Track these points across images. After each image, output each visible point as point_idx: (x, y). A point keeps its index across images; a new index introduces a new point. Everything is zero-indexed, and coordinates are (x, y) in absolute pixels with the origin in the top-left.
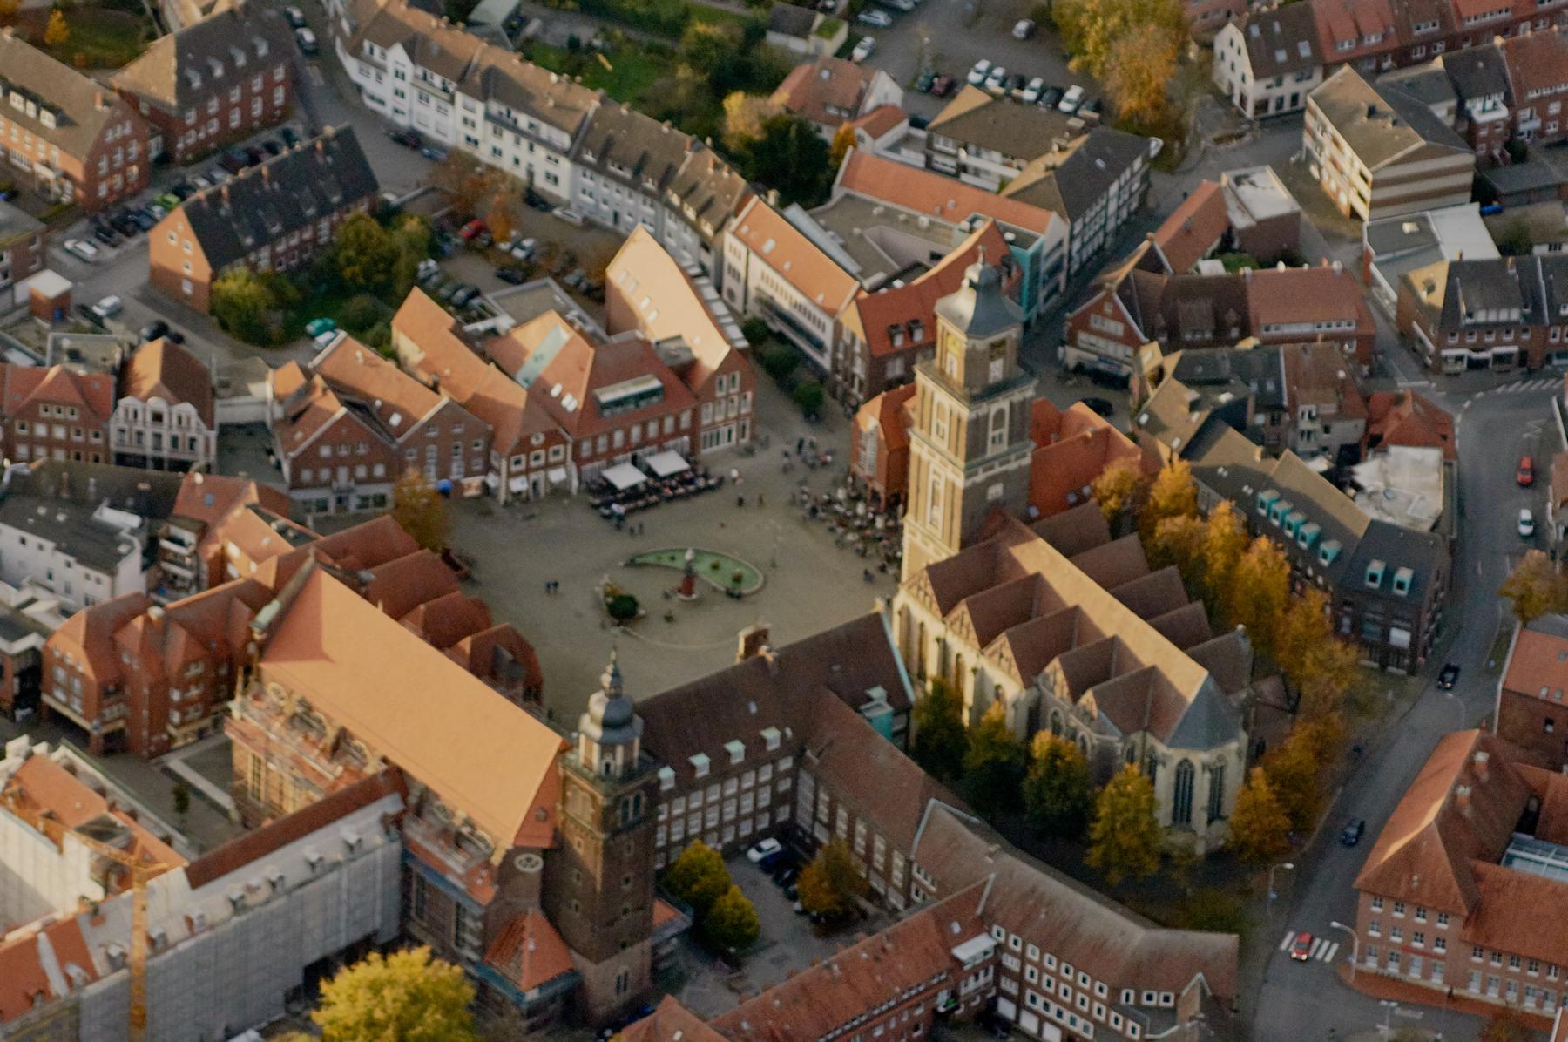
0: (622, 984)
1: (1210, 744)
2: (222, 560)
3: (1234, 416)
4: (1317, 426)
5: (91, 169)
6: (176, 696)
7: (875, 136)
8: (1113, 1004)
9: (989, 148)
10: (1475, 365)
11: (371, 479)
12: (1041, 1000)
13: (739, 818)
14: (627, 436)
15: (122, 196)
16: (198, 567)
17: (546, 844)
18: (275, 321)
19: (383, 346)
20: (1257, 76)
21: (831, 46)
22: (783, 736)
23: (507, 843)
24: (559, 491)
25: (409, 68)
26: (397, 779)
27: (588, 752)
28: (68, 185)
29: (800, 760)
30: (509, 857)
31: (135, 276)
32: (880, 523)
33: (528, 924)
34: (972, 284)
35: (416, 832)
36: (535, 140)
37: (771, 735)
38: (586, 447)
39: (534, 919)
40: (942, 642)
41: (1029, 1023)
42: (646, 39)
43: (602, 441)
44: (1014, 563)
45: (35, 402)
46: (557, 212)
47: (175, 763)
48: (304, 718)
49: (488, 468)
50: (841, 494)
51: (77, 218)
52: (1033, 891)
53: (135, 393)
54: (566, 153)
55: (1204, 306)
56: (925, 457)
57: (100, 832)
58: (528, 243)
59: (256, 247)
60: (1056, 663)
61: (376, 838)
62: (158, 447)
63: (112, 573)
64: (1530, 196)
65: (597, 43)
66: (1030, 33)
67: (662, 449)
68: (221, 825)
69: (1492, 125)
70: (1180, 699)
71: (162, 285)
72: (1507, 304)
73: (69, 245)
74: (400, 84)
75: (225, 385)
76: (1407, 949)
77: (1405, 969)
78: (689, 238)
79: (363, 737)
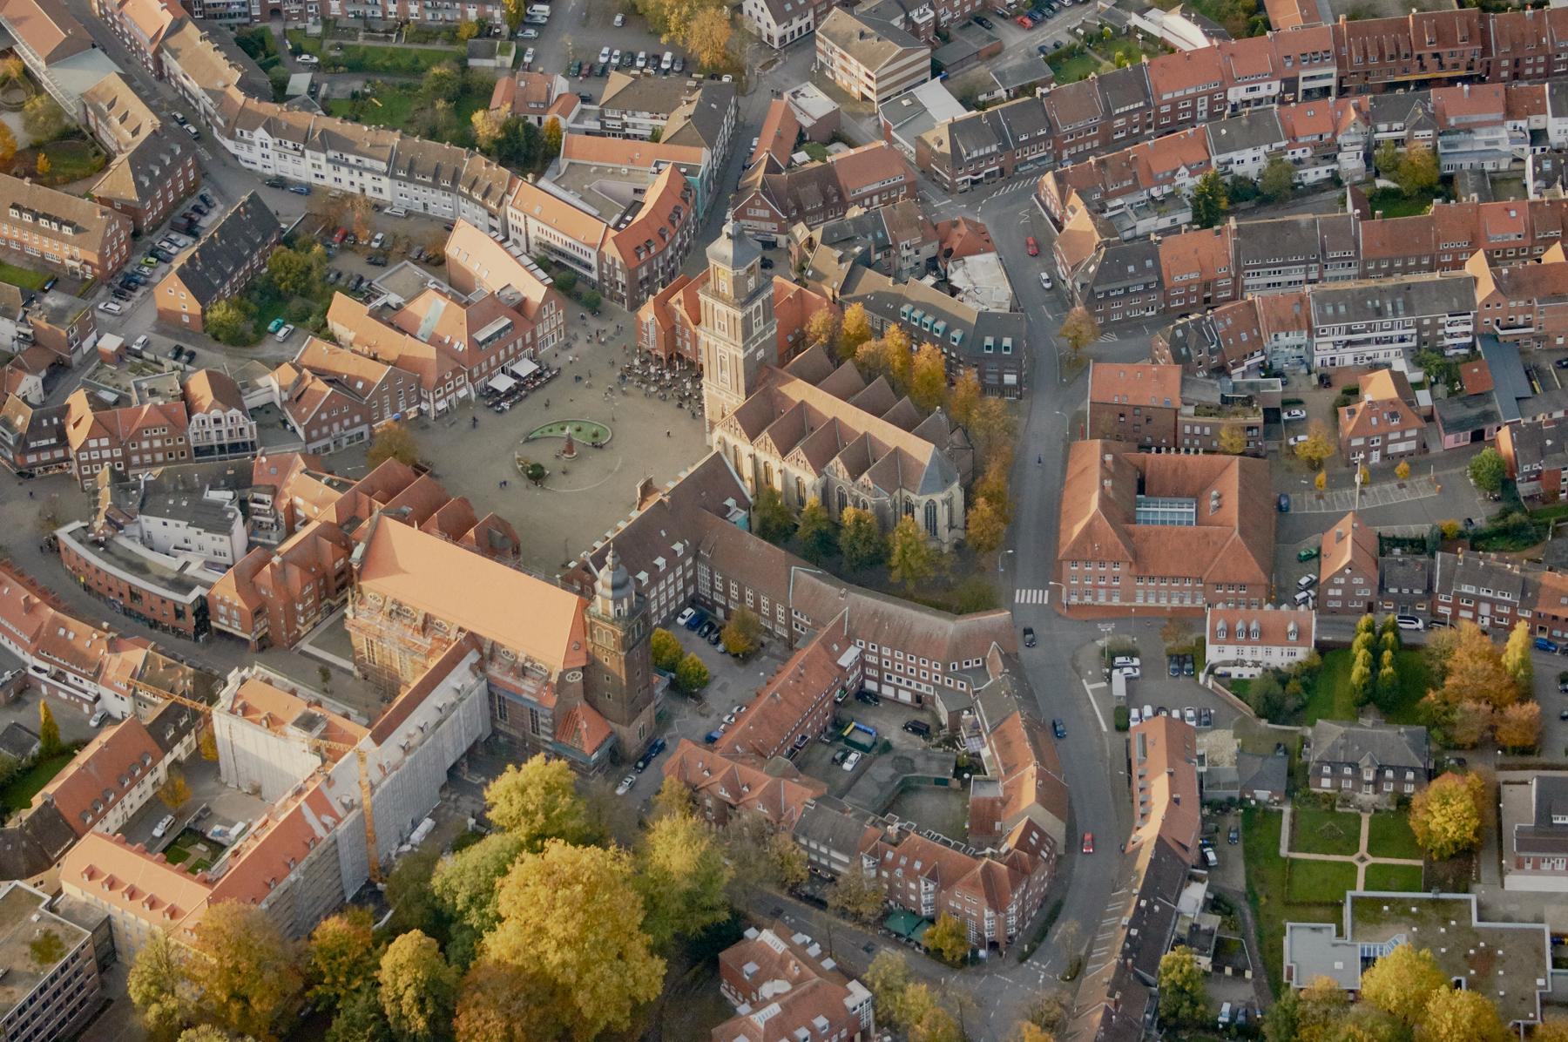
0: (642, 732)
1: (943, 489)
2: (292, 507)
3: (865, 261)
4: (912, 252)
5: (102, 256)
6: (300, 608)
7: (566, 117)
8: (945, 674)
9: (641, 111)
10: (974, 182)
11: (353, 425)
12: (894, 678)
13: (668, 601)
14: (498, 357)
15: (119, 267)
16: (276, 515)
17: (583, 663)
18: (248, 328)
19: (322, 331)
20: (778, 24)
21: (509, 61)
22: (685, 547)
23: (558, 668)
24: (465, 402)
25: (270, 141)
26: (474, 640)
27: (603, 603)
28: (89, 268)
29: (697, 557)
30: (562, 676)
31: (147, 318)
32: (668, 376)
33: (579, 711)
34: (729, 236)
35: (494, 671)
36: (362, 170)
37: (678, 547)
38: (476, 371)
39: (581, 704)
40: (753, 457)
41: (888, 691)
42: (398, 80)
43: (484, 365)
44: (784, 396)
45: (139, 429)
46: (387, 210)
47: (306, 646)
48: (398, 612)
49: (420, 399)
50: (637, 362)
51: (99, 287)
52: (875, 613)
53: (200, 407)
54: (386, 174)
55: (815, 187)
56: (712, 343)
57: (307, 723)
58: (379, 236)
59: (222, 284)
60: (837, 459)
61: (472, 681)
62: (220, 438)
63: (230, 535)
64: (963, 62)
65: (368, 91)
66: (624, 21)
67: (518, 359)
68: (349, 682)
69: (926, 23)
70: (921, 465)
71: (167, 322)
72: (990, 144)
73: (101, 306)
74: (265, 151)
75: (245, 386)
76: (1096, 587)
77: (1095, 598)
78: (482, 213)
79: (441, 615)
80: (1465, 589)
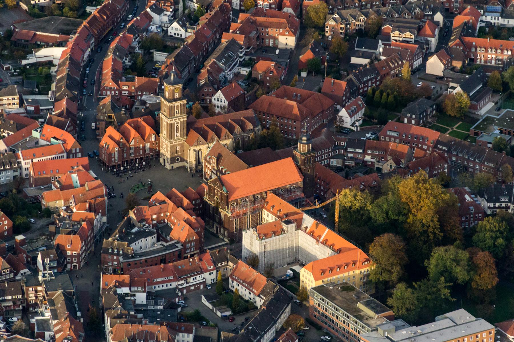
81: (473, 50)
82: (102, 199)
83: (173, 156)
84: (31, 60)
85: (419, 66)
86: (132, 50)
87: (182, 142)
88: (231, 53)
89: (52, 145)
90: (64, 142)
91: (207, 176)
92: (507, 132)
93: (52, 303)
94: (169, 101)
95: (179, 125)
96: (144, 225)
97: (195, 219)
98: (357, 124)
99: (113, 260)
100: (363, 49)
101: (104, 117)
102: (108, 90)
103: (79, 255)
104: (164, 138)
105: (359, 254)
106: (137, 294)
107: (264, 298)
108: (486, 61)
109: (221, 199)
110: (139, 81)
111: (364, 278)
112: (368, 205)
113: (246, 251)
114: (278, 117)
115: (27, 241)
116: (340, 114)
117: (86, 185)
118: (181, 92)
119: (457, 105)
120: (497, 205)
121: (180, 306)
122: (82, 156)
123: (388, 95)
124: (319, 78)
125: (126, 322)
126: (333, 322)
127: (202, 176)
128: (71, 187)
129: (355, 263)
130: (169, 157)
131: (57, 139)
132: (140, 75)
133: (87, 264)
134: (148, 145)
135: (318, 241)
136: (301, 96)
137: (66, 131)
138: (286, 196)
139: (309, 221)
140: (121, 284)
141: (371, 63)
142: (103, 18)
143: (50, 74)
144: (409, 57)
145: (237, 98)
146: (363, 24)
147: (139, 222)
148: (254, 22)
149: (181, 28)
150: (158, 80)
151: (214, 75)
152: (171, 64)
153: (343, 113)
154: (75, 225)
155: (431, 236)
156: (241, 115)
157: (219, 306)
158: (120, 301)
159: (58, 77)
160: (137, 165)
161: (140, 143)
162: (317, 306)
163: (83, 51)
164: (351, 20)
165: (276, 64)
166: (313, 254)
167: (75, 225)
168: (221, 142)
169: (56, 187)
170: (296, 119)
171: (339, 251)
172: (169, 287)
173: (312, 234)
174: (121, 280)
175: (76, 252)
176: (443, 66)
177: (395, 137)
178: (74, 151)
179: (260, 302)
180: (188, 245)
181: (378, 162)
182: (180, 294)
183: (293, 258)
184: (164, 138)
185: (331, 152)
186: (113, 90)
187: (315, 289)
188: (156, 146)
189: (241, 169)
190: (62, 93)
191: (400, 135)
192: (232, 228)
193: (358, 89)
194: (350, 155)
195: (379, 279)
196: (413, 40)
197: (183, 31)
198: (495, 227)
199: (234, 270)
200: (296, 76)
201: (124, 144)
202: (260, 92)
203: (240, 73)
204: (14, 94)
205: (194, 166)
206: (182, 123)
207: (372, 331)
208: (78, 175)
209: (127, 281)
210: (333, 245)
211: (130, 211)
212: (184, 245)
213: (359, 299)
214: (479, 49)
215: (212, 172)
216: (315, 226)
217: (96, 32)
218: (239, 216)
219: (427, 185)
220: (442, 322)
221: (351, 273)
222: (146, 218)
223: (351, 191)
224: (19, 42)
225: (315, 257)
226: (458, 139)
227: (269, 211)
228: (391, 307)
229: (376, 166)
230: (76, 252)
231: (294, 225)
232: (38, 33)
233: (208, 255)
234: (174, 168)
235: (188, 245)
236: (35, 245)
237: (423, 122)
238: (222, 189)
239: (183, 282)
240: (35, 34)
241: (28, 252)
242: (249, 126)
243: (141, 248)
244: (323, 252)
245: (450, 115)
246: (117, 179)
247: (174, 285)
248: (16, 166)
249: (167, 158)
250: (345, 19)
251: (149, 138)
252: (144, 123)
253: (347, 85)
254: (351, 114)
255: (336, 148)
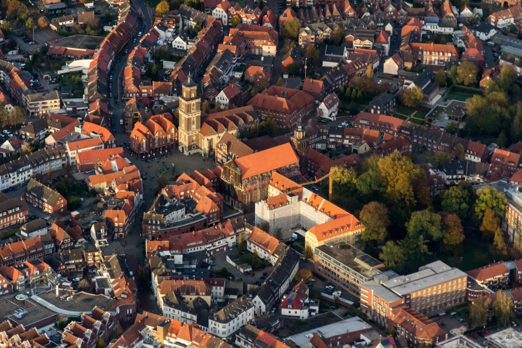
80: (336, 79)
81: (420, 53)
82: (138, 180)
83: (190, 144)
84: (65, 70)
85: (378, 67)
86: (146, 61)
87: (197, 133)
88: (227, 61)
89: (92, 138)
90: (102, 135)
91: (219, 160)
92: (454, 118)
93: (108, 265)
94: (187, 100)
95: (195, 119)
96: (174, 201)
97: (216, 195)
98: (334, 115)
99: (152, 229)
100: (332, 55)
101: (131, 115)
102: (131, 93)
103: (124, 226)
104: (182, 130)
105: (351, 219)
106: (175, 256)
107: (278, 256)
108: (430, 62)
109: (236, 178)
110: (156, 85)
111: (356, 238)
112: (354, 179)
113: (258, 219)
114: (271, 111)
115: (81, 216)
116: (320, 107)
117: (124, 170)
118: (196, 92)
119: (413, 98)
120: (455, 177)
121: (209, 265)
122: (117, 147)
123: (357, 91)
124: (298, 79)
125: (171, 279)
126: (335, 274)
127: (214, 160)
128: (111, 171)
129: (349, 226)
130: (187, 146)
131: (96, 133)
132: (157, 80)
133: (130, 233)
134: (169, 136)
135: (316, 209)
136: (287, 93)
137: (102, 126)
138: (287, 174)
139: (308, 194)
140: (163, 249)
141: (340, 66)
142: (120, 35)
143: (81, 81)
144: (370, 60)
145: (236, 97)
146: (329, 34)
147: (170, 198)
148: (243, 35)
149: (183, 41)
150: (171, 84)
151: (214, 78)
152: (180, 70)
153: (322, 106)
154: (119, 202)
155: (408, 202)
156: (243, 110)
157: (241, 264)
158: (164, 262)
159: (89, 84)
160: (161, 153)
161: (163, 135)
162: (321, 262)
163: (106, 62)
164: (320, 32)
165: (264, 69)
166: (313, 220)
167: (119, 202)
168: (229, 132)
169: (99, 172)
170: (285, 112)
171: (335, 217)
172: (199, 250)
173: (311, 204)
174: (162, 245)
175: (121, 224)
176: (397, 67)
177: (366, 125)
178: (110, 143)
179: (274, 260)
180: (211, 216)
181: (355, 145)
182: (209, 255)
183: (296, 224)
184: (182, 130)
185: (317, 138)
186: (135, 93)
187: (319, 248)
188: (175, 137)
189: (248, 153)
190: (94, 96)
191: (371, 123)
192: (245, 200)
193: (331, 87)
194: (331, 140)
195: (369, 239)
196: (371, 46)
197: (185, 43)
198: (459, 194)
199: (250, 235)
200: (280, 78)
201: (150, 136)
202: (253, 91)
203: (234, 76)
204: (56, 98)
205: (207, 152)
206: (197, 117)
207: (369, 280)
208: (116, 162)
209: (167, 246)
210: (329, 212)
211: (163, 190)
212: (208, 215)
213: (355, 255)
214: (425, 53)
215: (223, 156)
216: (314, 197)
217: (115, 46)
218: (250, 191)
219: (402, 162)
220: (424, 272)
221: (346, 234)
222: (176, 194)
223: (339, 169)
224: (53, 56)
225: (315, 222)
226: (418, 125)
227: (274, 187)
228: (382, 261)
229: (353, 148)
230: (121, 224)
231: (297, 197)
232: (69, 48)
233: (229, 223)
234: (191, 154)
235: (211, 216)
236: (87, 219)
237: (387, 112)
238: (236, 170)
239: (210, 245)
240: (66, 49)
241: (83, 225)
242: (250, 118)
243: (173, 219)
244: (321, 218)
245: (407, 106)
246: (147, 165)
247: (203, 248)
248: (64, 156)
249: (186, 146)
250: (314, 31)
251: (170, 131)
252: (164, 119)
253: (324, 84)
254: (329, 107)
255: (320, 134)
